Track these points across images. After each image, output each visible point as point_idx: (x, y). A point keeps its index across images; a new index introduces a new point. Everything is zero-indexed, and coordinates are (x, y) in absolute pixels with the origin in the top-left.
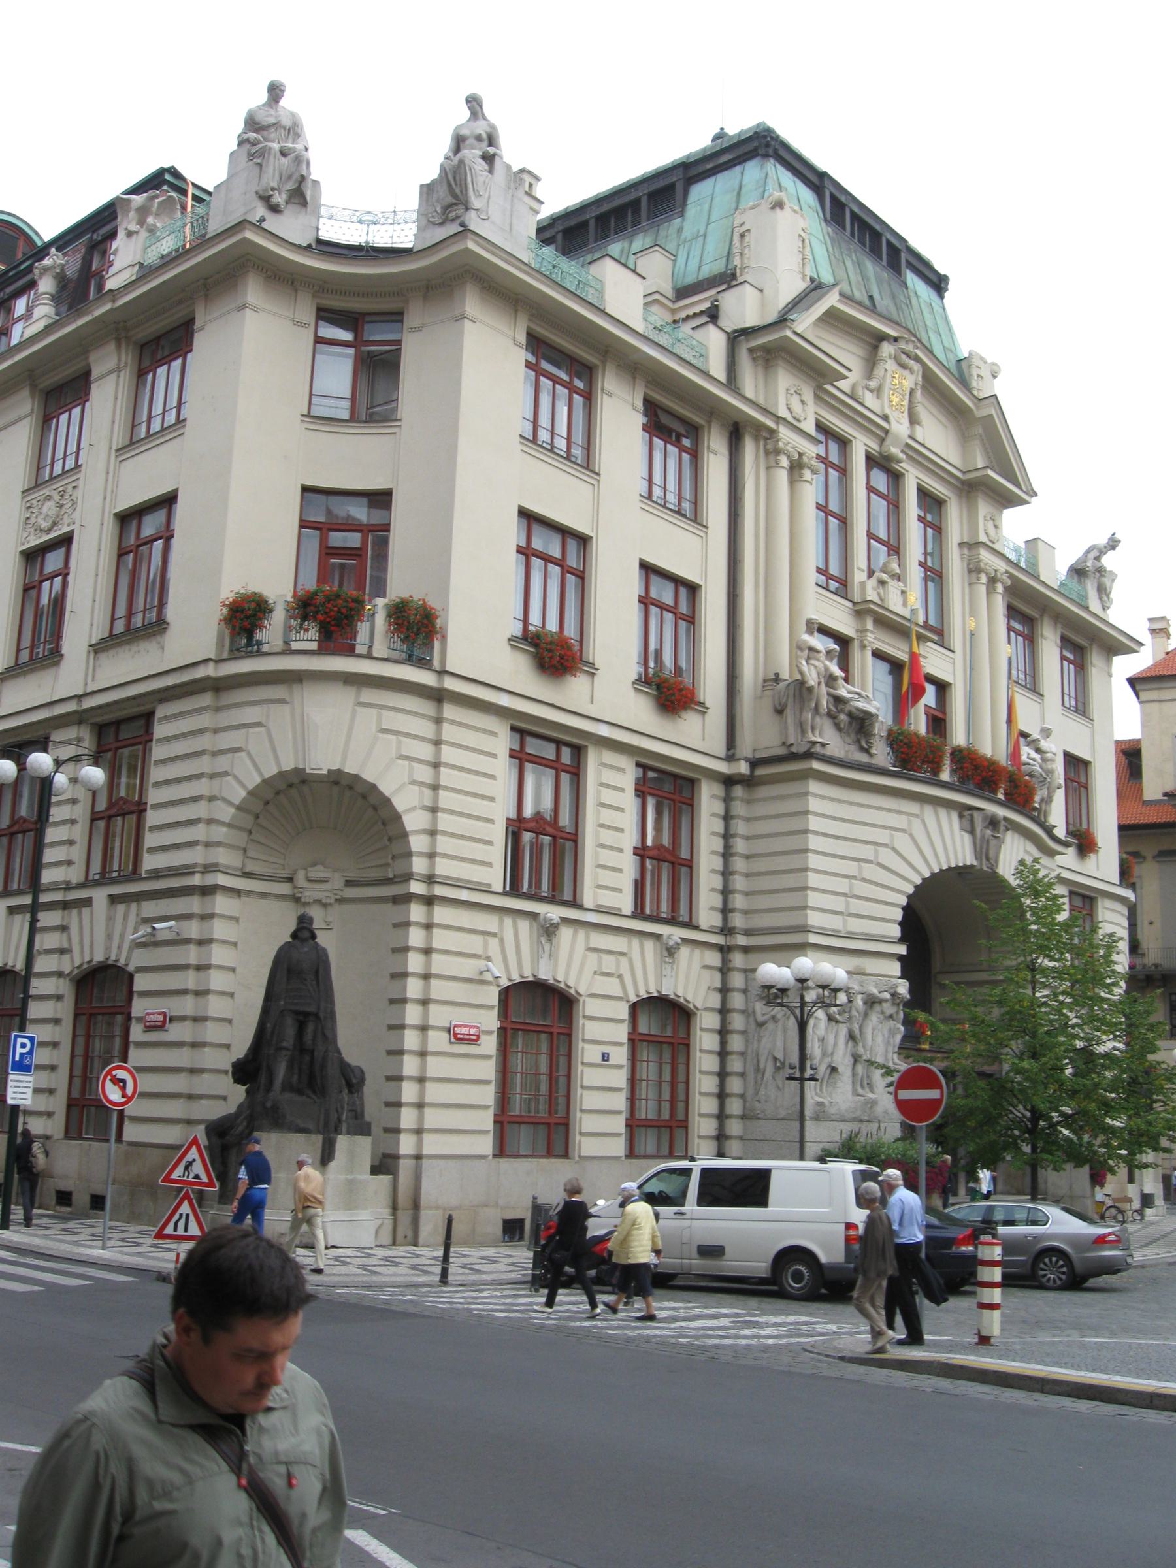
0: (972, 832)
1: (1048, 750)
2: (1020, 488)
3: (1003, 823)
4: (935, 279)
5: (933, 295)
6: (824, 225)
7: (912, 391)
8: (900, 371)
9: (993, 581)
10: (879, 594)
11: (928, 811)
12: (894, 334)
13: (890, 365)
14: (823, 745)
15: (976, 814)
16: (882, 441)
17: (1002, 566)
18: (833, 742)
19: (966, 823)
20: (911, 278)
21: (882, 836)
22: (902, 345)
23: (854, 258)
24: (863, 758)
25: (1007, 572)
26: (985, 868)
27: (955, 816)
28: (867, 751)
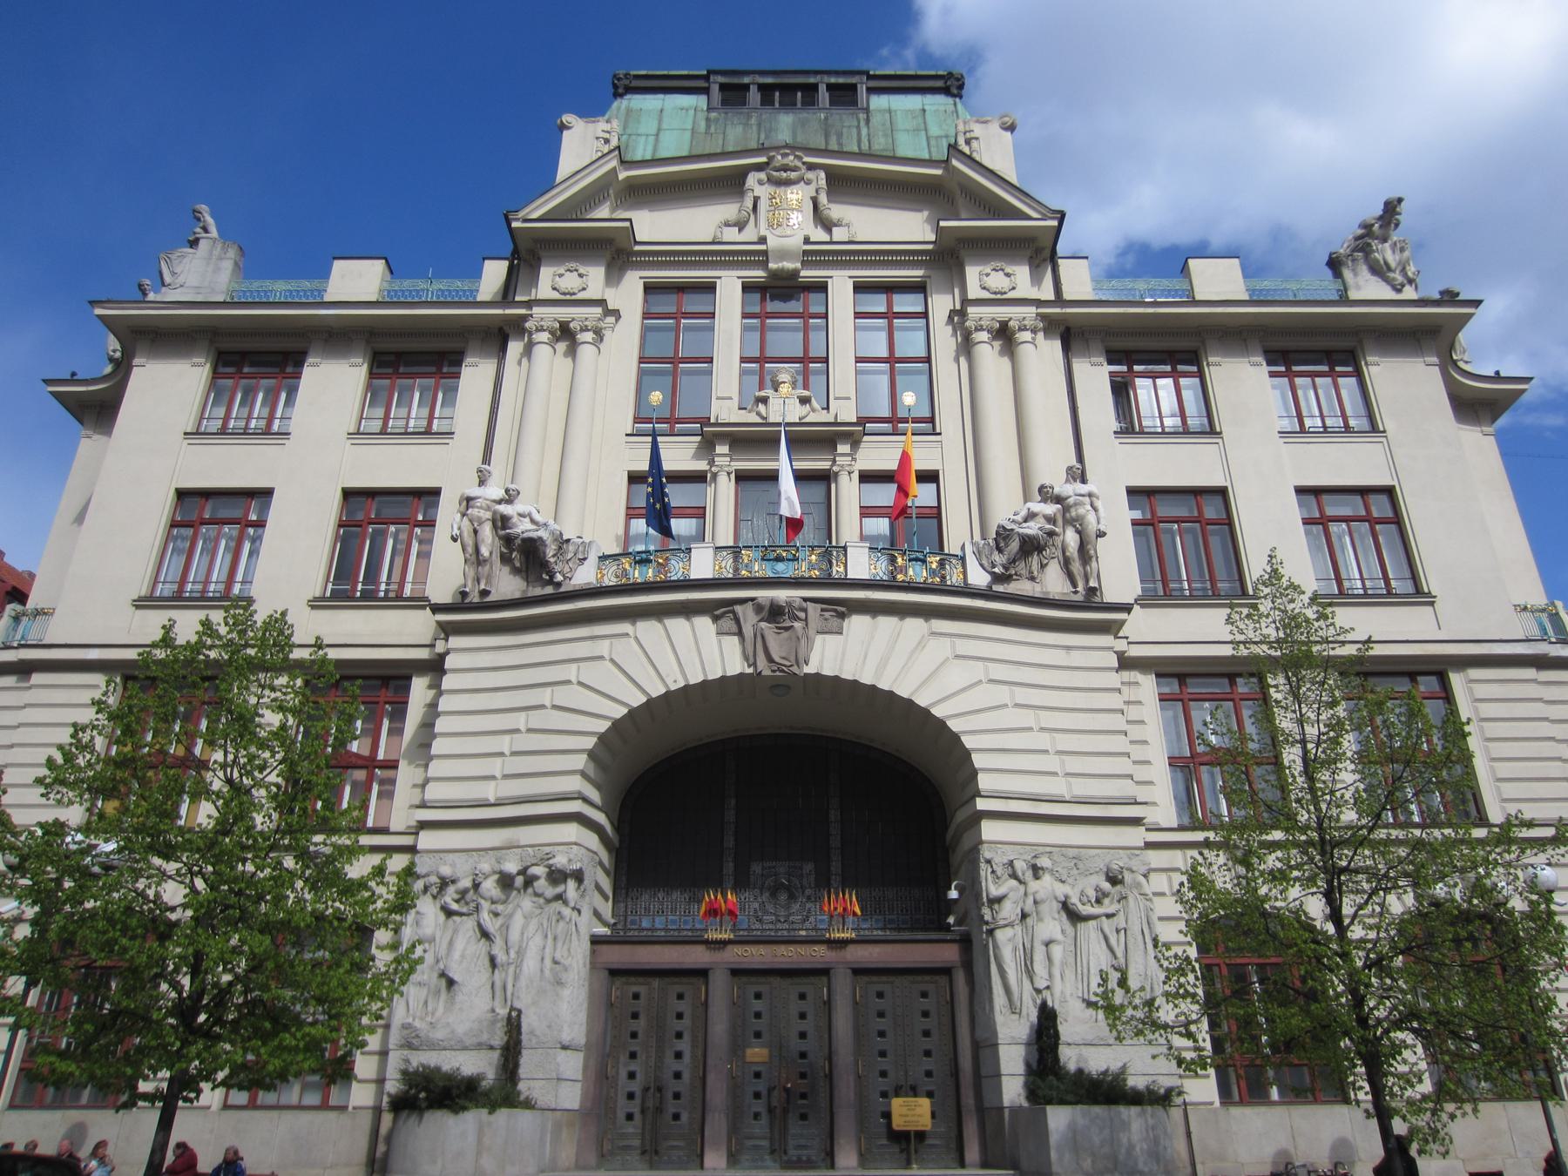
0: (740, 633)
1: (1071, 493)
2: (1030, 218)
3: (810, 605)
4: (940, 84)
6: (702, 117)
9: (1004, 335)
10: (759, 414)
11: (647, 629)
12: (764, 159)
13: (763, 192)
14: (485, 593)
15: (738, 608)
16: (767, 261)
17: (1033, 310)
18: (507, 584)
19: (727, 623)
20: (879, 102)
21: (571, 672)
24: (549, 590)
25: (1038, 314)
26: (767, 672)
27: (704, 623)
28: (551, 582)
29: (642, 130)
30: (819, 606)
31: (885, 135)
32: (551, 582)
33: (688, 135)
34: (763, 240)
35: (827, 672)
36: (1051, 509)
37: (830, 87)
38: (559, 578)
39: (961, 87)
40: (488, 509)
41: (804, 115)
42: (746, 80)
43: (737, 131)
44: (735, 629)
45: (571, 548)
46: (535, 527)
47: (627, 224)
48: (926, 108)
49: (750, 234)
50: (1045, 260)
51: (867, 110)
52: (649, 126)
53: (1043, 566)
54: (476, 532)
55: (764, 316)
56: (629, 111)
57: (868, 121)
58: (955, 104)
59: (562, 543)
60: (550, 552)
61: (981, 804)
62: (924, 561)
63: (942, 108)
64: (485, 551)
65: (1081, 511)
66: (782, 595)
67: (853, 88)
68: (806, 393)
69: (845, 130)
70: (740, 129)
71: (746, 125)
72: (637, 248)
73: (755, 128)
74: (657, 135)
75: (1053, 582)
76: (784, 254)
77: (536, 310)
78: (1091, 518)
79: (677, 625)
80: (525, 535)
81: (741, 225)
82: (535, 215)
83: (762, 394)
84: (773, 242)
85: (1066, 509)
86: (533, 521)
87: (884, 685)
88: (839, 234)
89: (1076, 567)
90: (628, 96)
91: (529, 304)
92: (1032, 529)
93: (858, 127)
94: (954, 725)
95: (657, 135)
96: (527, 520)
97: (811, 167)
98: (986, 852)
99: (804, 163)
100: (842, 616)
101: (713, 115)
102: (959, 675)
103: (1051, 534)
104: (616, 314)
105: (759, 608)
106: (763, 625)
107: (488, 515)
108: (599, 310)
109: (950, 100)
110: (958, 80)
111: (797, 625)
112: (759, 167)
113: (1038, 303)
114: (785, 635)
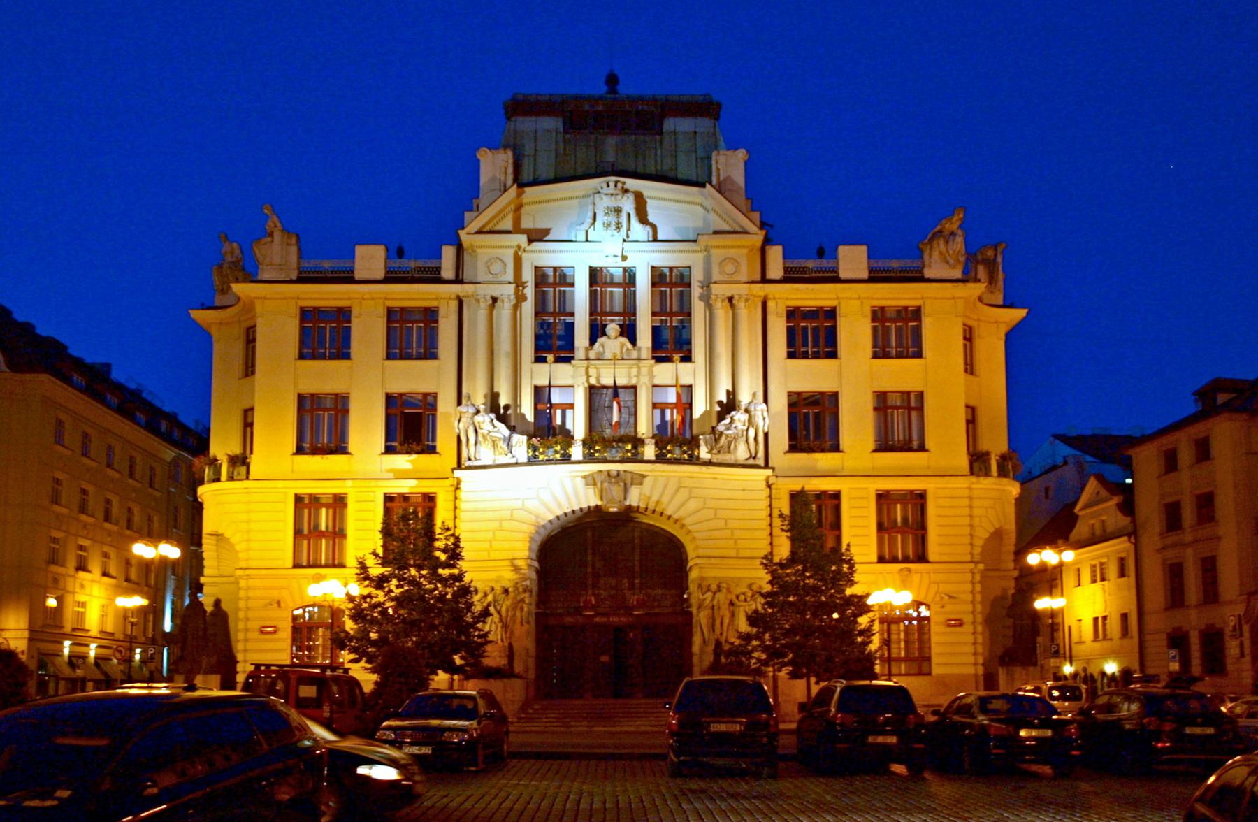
6: (560, 137)
20: (669, 124)
33: (553, 153)
35: (634, 504)
51: (661, 133)
57: (661, 142)
58: (715, 127)
74: (535, 155)
85: (750, 417)
90: (513, 119)
95: (535, 155)
101: (568, 136)
109: (713, 121)
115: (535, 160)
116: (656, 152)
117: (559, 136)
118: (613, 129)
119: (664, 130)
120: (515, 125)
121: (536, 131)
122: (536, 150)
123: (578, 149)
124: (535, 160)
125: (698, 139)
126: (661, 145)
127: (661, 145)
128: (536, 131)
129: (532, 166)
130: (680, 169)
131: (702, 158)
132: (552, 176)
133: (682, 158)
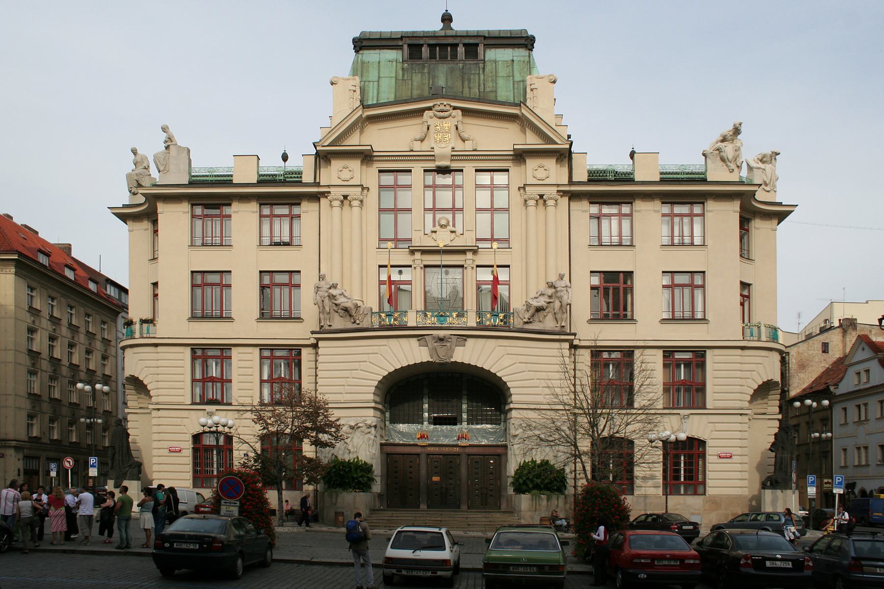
0: (427, 346)
4: (523, 42)
5: (519, 54)
6: (400, 66)
7: (457, 128)
8: (442, 120)
13: (433, 122)
14: (330, 326)
15: (426, 337)
17: (555, 189)
19: (422, 342)
20: (492, 54)
22: (437, 108)
23: (426, 70)
24: (355, 326)
25: (558, 191)
26: (437, 361)
27: (414, 341)
29: (370, 79)
30: (456, 336)
31: (492, 80)
32: (355, 322)
33: (394, 79)
34: (433, 148)
35: (459, 361)
36: (550, 291)
37: (465, 45)
38: (358, 322)
39: (532, 45)
40: (327, 292)
41: (452, 65)
42: (422, 42)
43: (418, 81)
44: (425, 344)
45: (362, 310)
46: (346, 300)
47: (369, 148)
48: (515, 59)
49: (425, 146)
50: (565, 157)
52: (373, 75)
53: (545, 316)
54: (323, 301)
55: (434, 187)
56: (363, 63)
57: (484, 69)
59: (357, 307)
60: (353, 313)
61: (512, 406)
62: (498, 316)
63: (522, 59)
64: (327, 309)
65: (562, 294)
66: (442, 333)
67: (477, 45)
68: (453, 229)
69: (472, 77)
70: (419, 76)
71: (422, 73)
72: (375, 154)
73: (427, 74)
74: (378, 81)
75: (549, 323)
76: (443, 157)
77: (332, 190)
78: (565, 297)
79: (403, 341)
80: (342, 305)
81: (422, 140)
82: (326, 144)
83: (434, 229)
84: (437, 151)
86: (345, 296)
87: (479, 365)
88: (468, 146)
89: (558, 316)
90: (361, 52)
91: (329, 186)
92: (542, 302)
93: (479, 74)
94: (504, 379)
96: (342, 296)
97: (455, 108)
98: (512, 421)
99: (451, 106)
100: (465, 340)
102: (507, 361)
103: (549, 303)
104: (368, 189)
105: (434, 338)
106: (435, 344)
107: (326, 294)
108: (360, 189)
109: (528, 51)
110: (532, 40)
111: (448, 344)
112: (430, 109)
113: (558, 185)
114: (445, 347)
115: (378, 85)
116: (479, 79)
117: (398, 64)
118: (443, 58)
119: (486, 59)
120: (362, 57)
121: (379, 62)
122: (379, 77)
123: (414, 74)
124: (378, 85)
125: (516, 67)
126: (484, 71)
127: (484, 71)
128: (379, 62)
129: (375, 91)
130: (499, 94)
131: (518, 82)
132: (392, 98)
133: (501, 82)
